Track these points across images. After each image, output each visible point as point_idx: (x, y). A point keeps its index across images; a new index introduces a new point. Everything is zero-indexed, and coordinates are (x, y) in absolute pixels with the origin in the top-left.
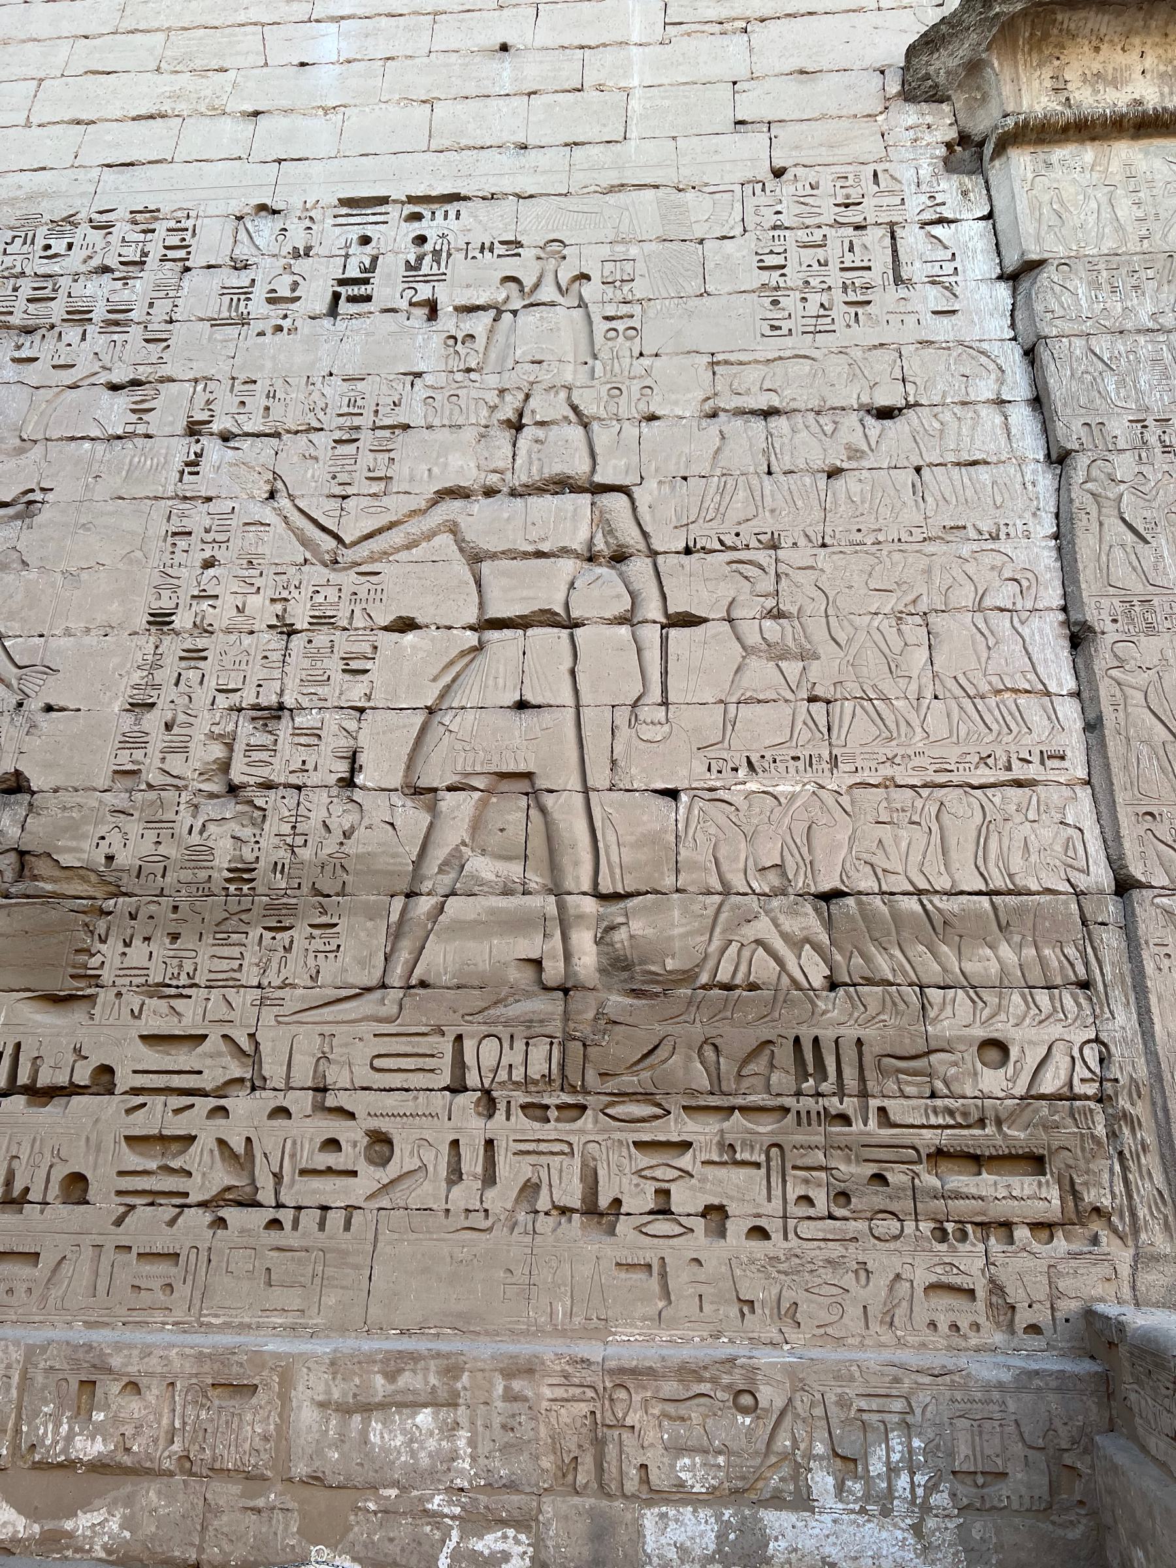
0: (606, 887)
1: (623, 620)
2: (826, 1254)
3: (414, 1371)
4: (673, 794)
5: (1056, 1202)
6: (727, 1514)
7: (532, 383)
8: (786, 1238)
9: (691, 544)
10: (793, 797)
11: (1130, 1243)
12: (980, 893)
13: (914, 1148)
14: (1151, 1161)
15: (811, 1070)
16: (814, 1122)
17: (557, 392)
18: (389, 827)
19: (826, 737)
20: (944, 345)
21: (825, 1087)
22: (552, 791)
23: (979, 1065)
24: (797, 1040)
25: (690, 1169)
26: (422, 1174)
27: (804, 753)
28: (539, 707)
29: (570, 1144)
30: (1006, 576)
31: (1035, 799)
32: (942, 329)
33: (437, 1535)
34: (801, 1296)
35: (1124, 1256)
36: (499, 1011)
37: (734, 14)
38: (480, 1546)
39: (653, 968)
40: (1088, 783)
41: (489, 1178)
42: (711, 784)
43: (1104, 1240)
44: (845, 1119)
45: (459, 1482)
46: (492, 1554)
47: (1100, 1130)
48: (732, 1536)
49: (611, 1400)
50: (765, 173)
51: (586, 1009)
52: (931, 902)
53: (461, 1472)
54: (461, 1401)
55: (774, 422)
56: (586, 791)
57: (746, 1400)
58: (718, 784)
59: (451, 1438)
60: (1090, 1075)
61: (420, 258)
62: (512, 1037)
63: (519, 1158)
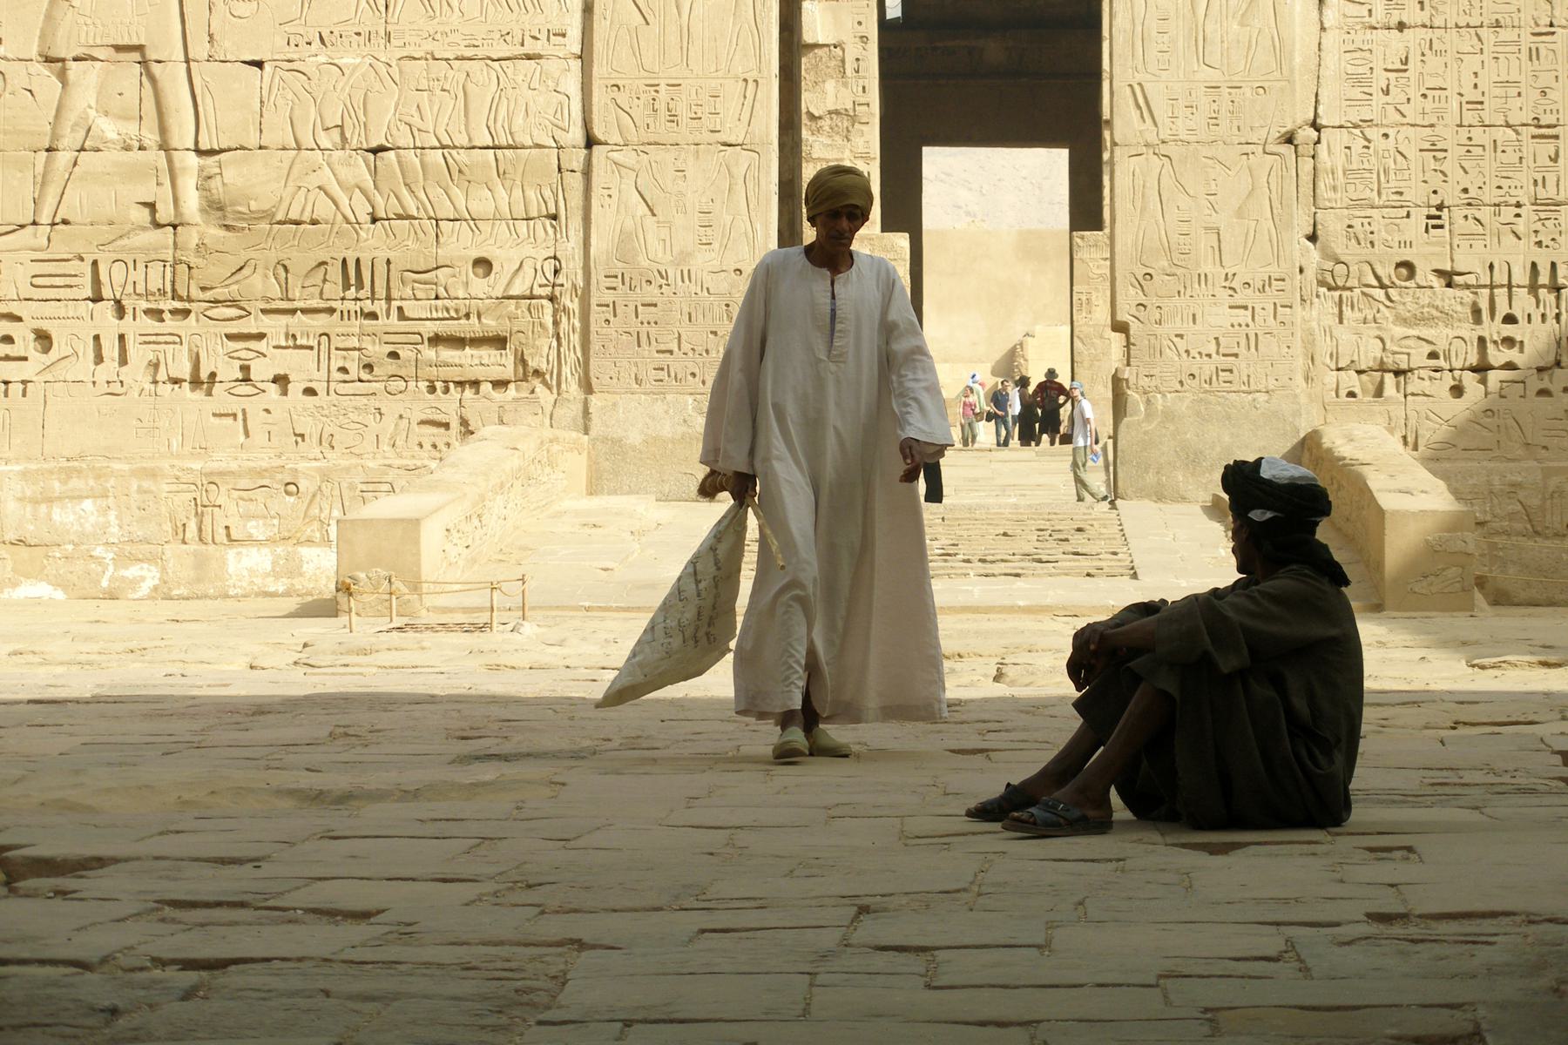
0: (205, 145)
2: (354, 403)
3: (78, 477)
4: (259, 64)
5: (511, 367)
6: (279, 550)
8: (328, 394)
10: (355, 68)
11: (555, 391)
12: (487, 148)
13: (419, 334)
14: (576, 339)
15: (353, 281)
16: (353, 317)
18: (28, 93)
19: (384, 15)
21: (362, 294)
22: (159, 62)
23: (471, 275)
24: (344, 261)
25: (264, 351)
26: (74, 358)
27: (363, 30)
29: (180, 337)
31: (538, 73)
36: (125, 241)
39: (240, 209)
40: (580, 57)
41: (123, 361)
42: (290, 56)
43: (537, 390)
44: (373, 316)
46: (134, 578)
47: (548, 320)
48: (281, 562)
49: (207, 491)
51: (190, 237)
52: (449, 153)
54: (110, 494)
56: (187, 61)
57: (292, 488)
58: (295, 56)
59: (105, 515)
60: (546, 282)
62: (135, 261)
63: (145, 346)
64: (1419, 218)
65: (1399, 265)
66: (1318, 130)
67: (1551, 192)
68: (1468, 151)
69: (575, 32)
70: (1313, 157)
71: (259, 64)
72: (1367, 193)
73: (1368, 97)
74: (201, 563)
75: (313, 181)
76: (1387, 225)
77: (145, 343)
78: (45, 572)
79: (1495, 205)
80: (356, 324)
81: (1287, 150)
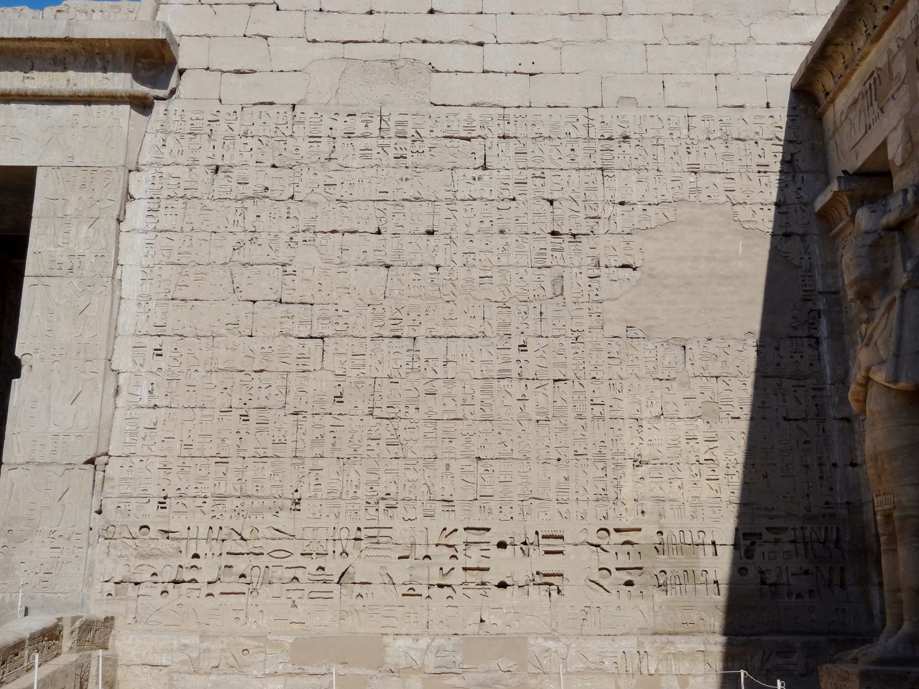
64: (154, 503)
65: (142, 527)
67: (222, 490)
70: (104, 471)
72: (129, 491)
73: (136, 442)
76: (138, 506)
81: (90, 467)
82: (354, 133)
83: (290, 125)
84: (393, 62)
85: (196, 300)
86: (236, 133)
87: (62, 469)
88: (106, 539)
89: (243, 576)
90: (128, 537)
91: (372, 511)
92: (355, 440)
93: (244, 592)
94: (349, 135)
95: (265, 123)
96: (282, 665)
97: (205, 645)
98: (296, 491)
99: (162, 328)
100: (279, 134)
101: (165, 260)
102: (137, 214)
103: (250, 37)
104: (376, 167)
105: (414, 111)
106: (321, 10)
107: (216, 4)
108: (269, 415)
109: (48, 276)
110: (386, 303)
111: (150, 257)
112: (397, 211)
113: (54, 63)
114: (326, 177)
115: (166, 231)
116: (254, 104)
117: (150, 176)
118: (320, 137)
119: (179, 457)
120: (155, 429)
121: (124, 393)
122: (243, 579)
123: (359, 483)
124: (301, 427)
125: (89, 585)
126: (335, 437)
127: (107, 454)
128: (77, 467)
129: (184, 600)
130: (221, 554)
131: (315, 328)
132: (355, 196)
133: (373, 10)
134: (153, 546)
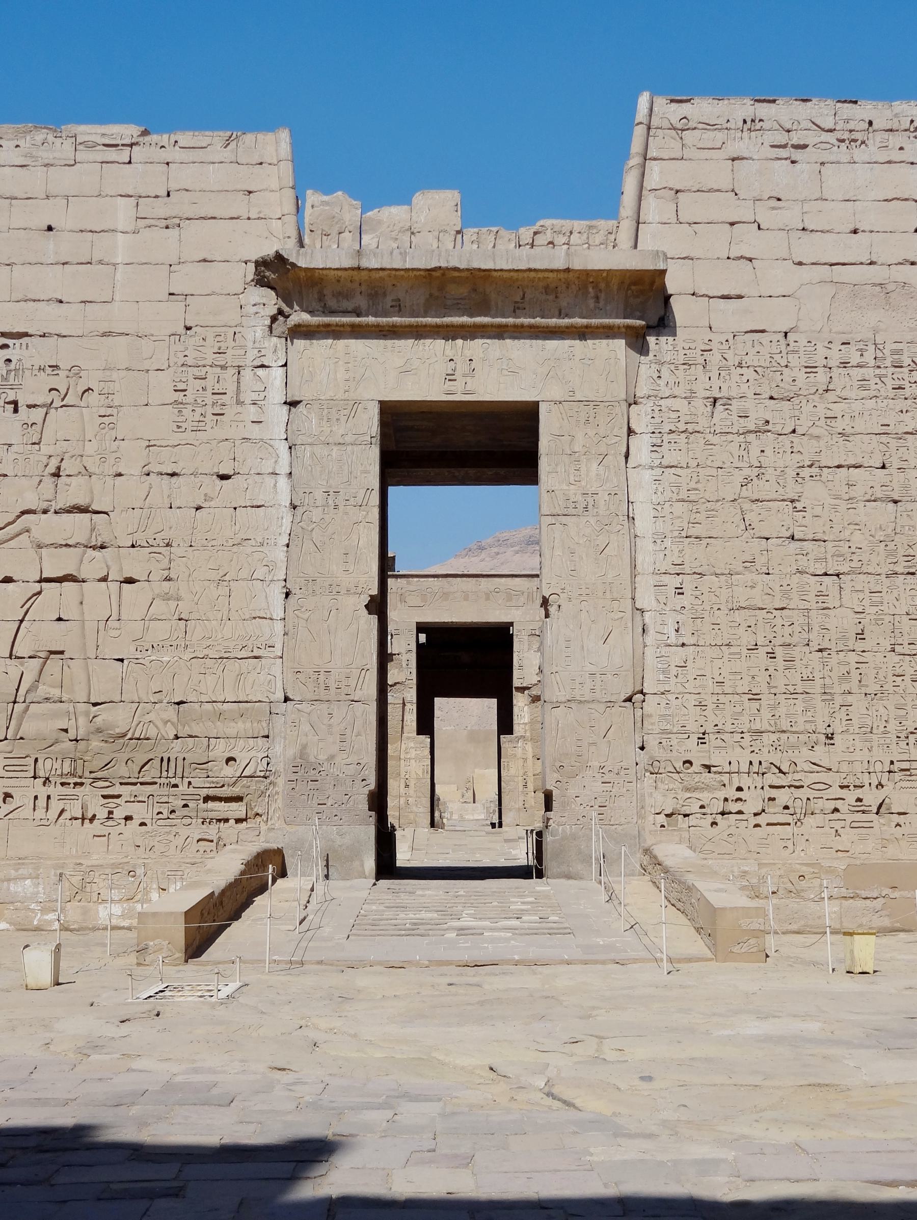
1: (104, 579)
2: (166, 830)
4: (122, 660)
6: (125, 905)
7: (65, 453)
9: (134, 543)
12: (235, 702)
17: (76, 458)
20: (254, 441)
22: (72, 659)
24: (162, 758)
27: (174, 644)
28: (68, 620)
30: (265, 564)
32: (255, 432)
33: (34, 915)
34: (156, 843)
35: (264, 827)
37: (174, 215)
38: (46, 917)
44: (176, 786)
45: (40, 900)
50: (182, 330)
53: (41, 897)
55: (175, 478)
58: (139, 657)
61: (9, 372)
64: (694, 738)
65: (685, 762)
66: (644, 696)
67: (757, 726)
68: (718, 706)
69: (279, 646)
70: (642, 708)
71: (122, 660)
72: (668, 727)
74: (85, 912)
75: (148, 718)
77: (60, 799)
78: (5, 917)
79: (731, 733)
80: (165, 790)
81: (628, 704)
82: (849, 363)
83: (784, 354)
84: (883, 286)
85: (709, 538)
86: (730, 363)
87: (602, 707)
88: (652, 773)
89: (786, 807)
90: (672, 771)
91: (903, 744)
92: (881, 676)
93: (788, 822)
94: (844, 364)
95: (758, 352)
96: (837, 889)
97: (763, 871)
98: (829, 726)
99: (680, 567)
100: (775, 364)
101: (675, 497)
102: (641, 447)
103: (733, 259)
104: (874, 400)
105: (909, 339)
106: (803, 229)
107: (695, 223)
108: (796, 652)
109: (564, 515)
110: (897, 538)
111: (659, 493)
112: (899, 445)
113: (546, 292)
114: (826, 410)
115: (671, 467)
116: (746, 332)
117: (650, 410)
118: (816, 367)
119: (713, 694)
120: (686, 667)
121: (651, 632)
122: (786, 811)
123: (888, 718)
124: (827, 663)
125: (640, 816)
126: (860, 674)
127: (641, 692)
128: (617, 705)
129: (733, 830)
130: (762, 788)
131: (830, 565)
132: (858, 429)
133: (858, 229)
134: (696, 780)
